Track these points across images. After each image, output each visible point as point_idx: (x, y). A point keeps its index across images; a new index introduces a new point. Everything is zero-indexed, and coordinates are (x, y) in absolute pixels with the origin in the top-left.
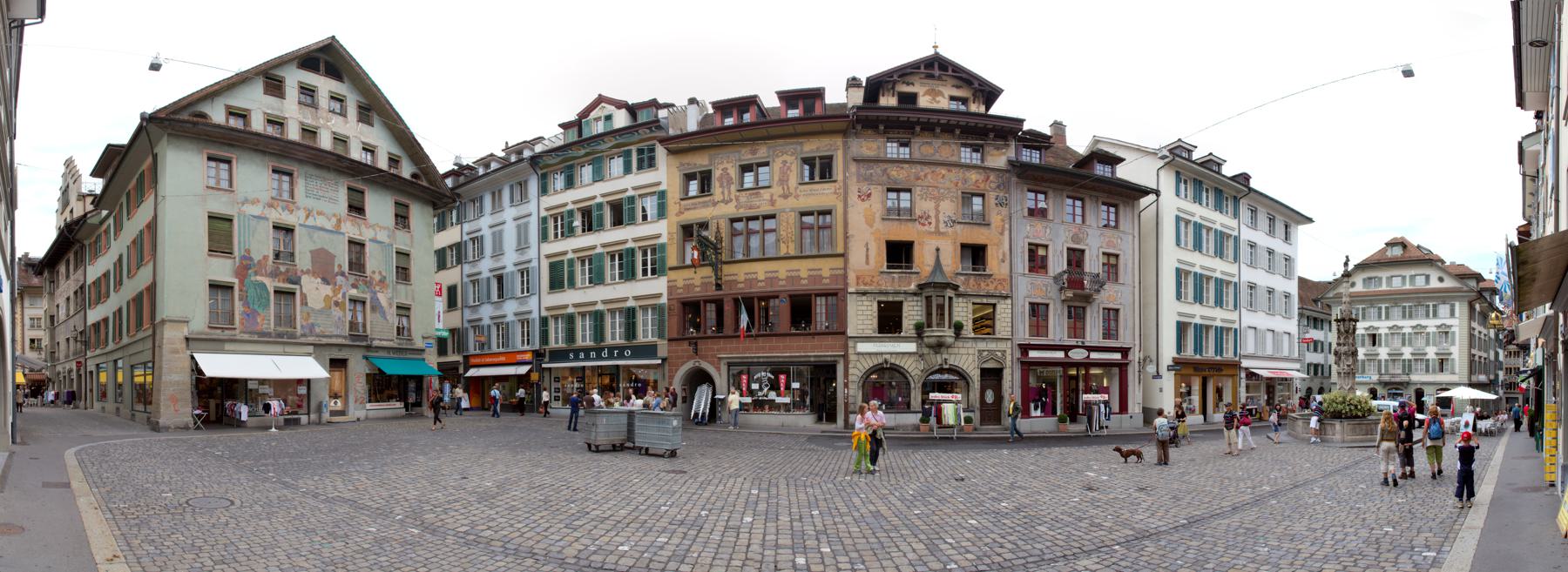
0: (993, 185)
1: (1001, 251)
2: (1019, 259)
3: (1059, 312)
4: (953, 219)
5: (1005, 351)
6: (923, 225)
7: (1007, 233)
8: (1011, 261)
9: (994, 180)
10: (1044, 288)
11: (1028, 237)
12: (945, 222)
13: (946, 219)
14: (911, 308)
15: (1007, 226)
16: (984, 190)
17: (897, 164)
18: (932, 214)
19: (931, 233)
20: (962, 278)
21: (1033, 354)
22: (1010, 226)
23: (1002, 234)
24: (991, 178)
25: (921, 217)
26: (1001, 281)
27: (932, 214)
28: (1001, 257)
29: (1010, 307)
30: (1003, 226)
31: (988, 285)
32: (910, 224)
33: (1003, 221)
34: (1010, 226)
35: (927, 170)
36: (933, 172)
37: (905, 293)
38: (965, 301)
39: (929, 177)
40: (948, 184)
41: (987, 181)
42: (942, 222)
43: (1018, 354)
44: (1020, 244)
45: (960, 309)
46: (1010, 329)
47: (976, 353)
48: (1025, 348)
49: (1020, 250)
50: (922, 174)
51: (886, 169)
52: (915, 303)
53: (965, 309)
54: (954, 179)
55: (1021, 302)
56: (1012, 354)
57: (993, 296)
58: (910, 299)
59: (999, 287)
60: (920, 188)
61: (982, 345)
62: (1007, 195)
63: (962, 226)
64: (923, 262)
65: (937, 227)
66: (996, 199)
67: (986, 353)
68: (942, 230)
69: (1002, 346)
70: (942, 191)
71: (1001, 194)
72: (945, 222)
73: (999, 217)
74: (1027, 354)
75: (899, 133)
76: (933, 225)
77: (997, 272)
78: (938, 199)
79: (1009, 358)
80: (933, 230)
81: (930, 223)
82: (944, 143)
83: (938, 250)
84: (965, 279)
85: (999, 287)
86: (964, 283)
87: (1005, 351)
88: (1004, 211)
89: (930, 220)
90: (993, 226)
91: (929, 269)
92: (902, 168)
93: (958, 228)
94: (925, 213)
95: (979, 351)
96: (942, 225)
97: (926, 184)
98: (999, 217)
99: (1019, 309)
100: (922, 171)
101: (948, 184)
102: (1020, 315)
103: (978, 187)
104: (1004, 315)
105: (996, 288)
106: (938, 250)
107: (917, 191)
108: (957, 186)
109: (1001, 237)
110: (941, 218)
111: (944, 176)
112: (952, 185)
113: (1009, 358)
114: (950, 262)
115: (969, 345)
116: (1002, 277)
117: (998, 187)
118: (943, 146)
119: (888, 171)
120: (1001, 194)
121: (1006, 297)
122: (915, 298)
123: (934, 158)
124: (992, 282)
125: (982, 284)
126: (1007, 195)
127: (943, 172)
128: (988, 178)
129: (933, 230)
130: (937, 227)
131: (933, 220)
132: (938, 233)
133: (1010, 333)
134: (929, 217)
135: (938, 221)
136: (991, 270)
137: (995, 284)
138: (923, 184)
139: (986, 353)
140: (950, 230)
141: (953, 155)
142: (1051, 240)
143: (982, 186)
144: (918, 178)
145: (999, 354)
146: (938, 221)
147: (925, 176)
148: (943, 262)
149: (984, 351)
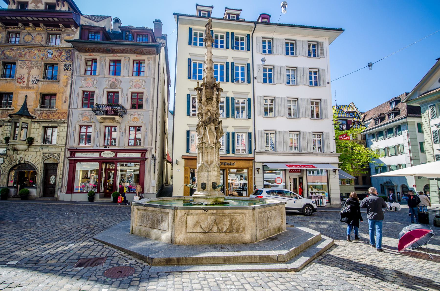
0: (64, 58)
1: (64, 96)
2: (75, 100)
3: (98, 130)
4: (37, 79)
5: (60, 154)
6: (20, 83)
7: (69, 86)
8: (70, 101)
9: (65, 55)
10: (89, 117)
11: (82, 87)
12: (33, 81)
13: (33, 79)
14: (6, 129)
15: (70, 82)
16: (58, 61)
17: (10, 48)
18: (26, 77)
19: (24, 87)
20: (39, 112)
21: (78, 155)
22: (72, 81)
23: (66, 86)
24: (63, 54)
25: (19, 79)
26: (62, 114)
27: (26, 77)
28: (64, 99)
29: (66, 128)
30: (67, 82)
31: (54, 116)
32: (12, 83)
33: (67, 78)
34: (72, 81)
35: (27, 51)
36: (29, 52)
37: (3, 121)
38: (38, 125)
39: (27, 55)
40: (37, 59)
41: (60, 56)
42: (31, 81)
43: (68, 155)
44: (77, 91)
45: (35, 130)
46: (65, 141)
47: (42, 155)
48: (73, 152)
49: (76, 95)
50: (23, 53)
51: (4, 51)
52: (9, 127)
53: (38, 130)
54: (41, 56)
55: (73, 125)
56: (65, 155)
57: (55, 122)
58: (6, 124)
59: (61, 117)
60: (21, 62)
61: (46, 150)
62: (71, 63)
63: (42, 83)
64: (17, 104)
65: (28, 84)
66: (65, 66)
67: (47, 154)
68: (30, 86)
69: (58, 151)
70: (33, 63)
71: (68, 63)
72: (33, 81)
73: (66, 77)
74: (74, 155)
75: (14, 28)
76: (25, 83)
77: (60, 108)
78: (30, 68)
79: (62, 157)
80: (25, 85)
81: (24, 82)
82: (38, 34)
83: (26, 96)
84: (41, 113)
85: (61, 117)
86: (39, 115)
87: (60, 154)
88: (69, 73)
89: (24, 80)
90: (61, 82)
91: (19, 108)
92: (13, 50)
93: (40, 84)
94: (22, 76)
95: (44, 153)
96: (30, 83)
97: (25, 59)
98: (66, 77)
99: (71, 129)
100: (23, 51)
101: (37, 59)
102: (72, 132)
103: (55, 59)
104: (63, 133)
105: (59, 118)
106: (26, 96)
107: (19, 63)
108: (42, 59)
109: (65, 88)
110: (31, 78)
111: (36, 54)
112: (40, 59)
113: (62, 157)
114: (32, 103)
115: (38, 150)
116: (63, 111)
117: (67, 59)
118: (37, 36)
119: (5, 51)
120: (68, 63)
121: (64, 122)
122: (9, 124)
123: (32, 43)
124: (57, 114)
125: (51, 116)
126: (71, 63)
127: (36, 52)
128: (61, 53)
129: (25, 85)
130: (28, 84)
131: (26, 80)
132: (28, 87)
133: (65, 143)
134: (24, 78)
135: (28, 80)
136: (57, 108)
137: (58, 115)
138: (23, 59)
139: (47, 154)
140: (35, 86)
141: (42, 41)
142: (96, 88)
143: (57, 59)
144: (21, 56)
145: (56, 155)
146: (28, 80)
147: (25, 54)
148: (28, 104)
149: (46, 153)
